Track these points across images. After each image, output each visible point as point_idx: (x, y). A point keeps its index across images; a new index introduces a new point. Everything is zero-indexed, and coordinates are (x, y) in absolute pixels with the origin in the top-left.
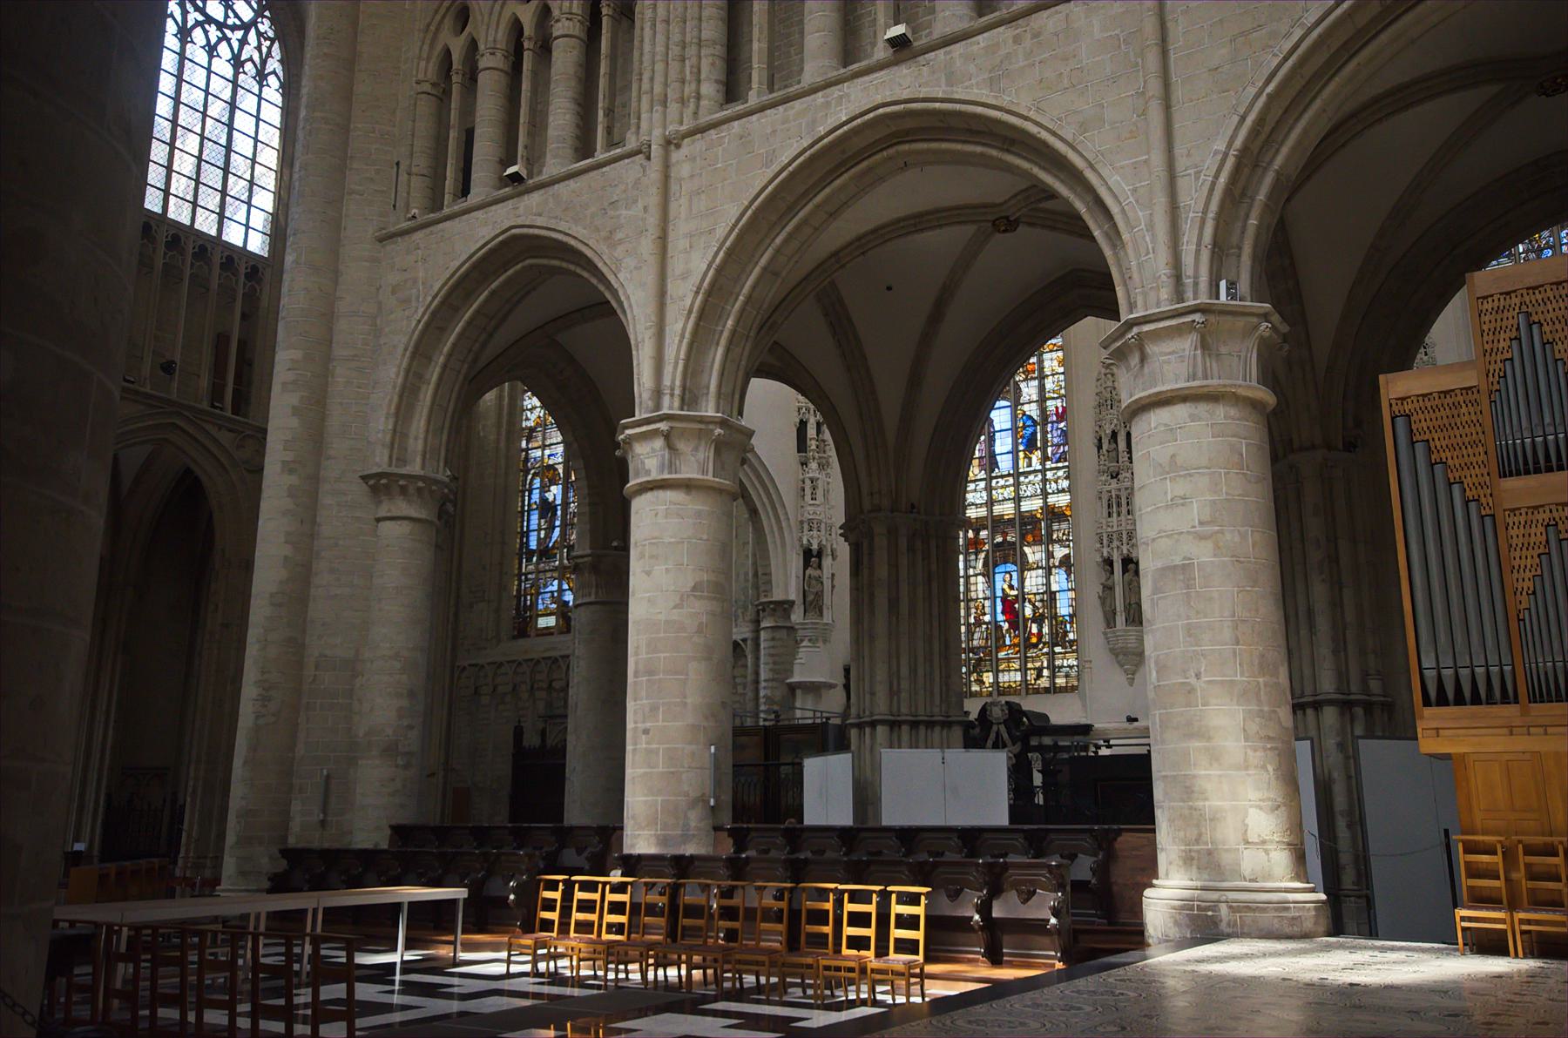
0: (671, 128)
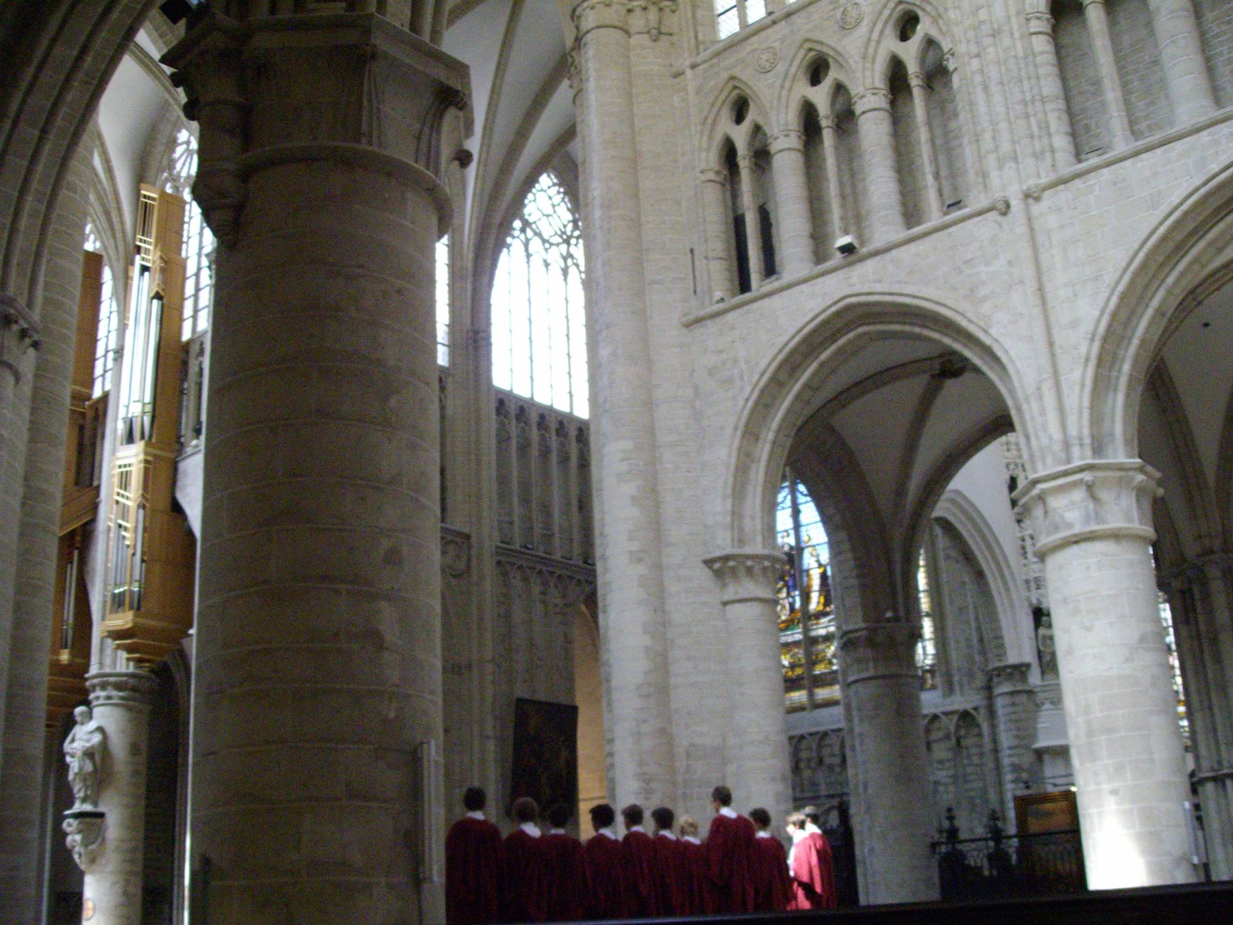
0: (1031, 183)
